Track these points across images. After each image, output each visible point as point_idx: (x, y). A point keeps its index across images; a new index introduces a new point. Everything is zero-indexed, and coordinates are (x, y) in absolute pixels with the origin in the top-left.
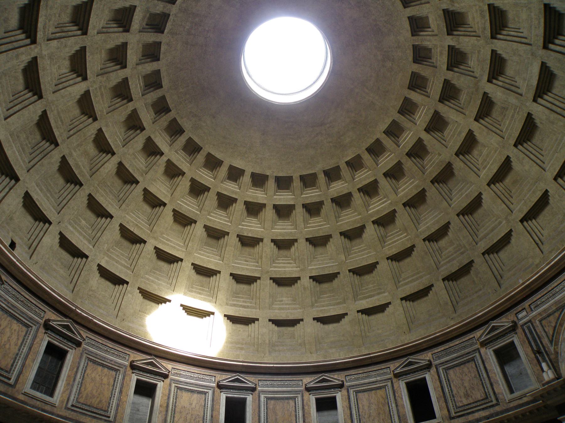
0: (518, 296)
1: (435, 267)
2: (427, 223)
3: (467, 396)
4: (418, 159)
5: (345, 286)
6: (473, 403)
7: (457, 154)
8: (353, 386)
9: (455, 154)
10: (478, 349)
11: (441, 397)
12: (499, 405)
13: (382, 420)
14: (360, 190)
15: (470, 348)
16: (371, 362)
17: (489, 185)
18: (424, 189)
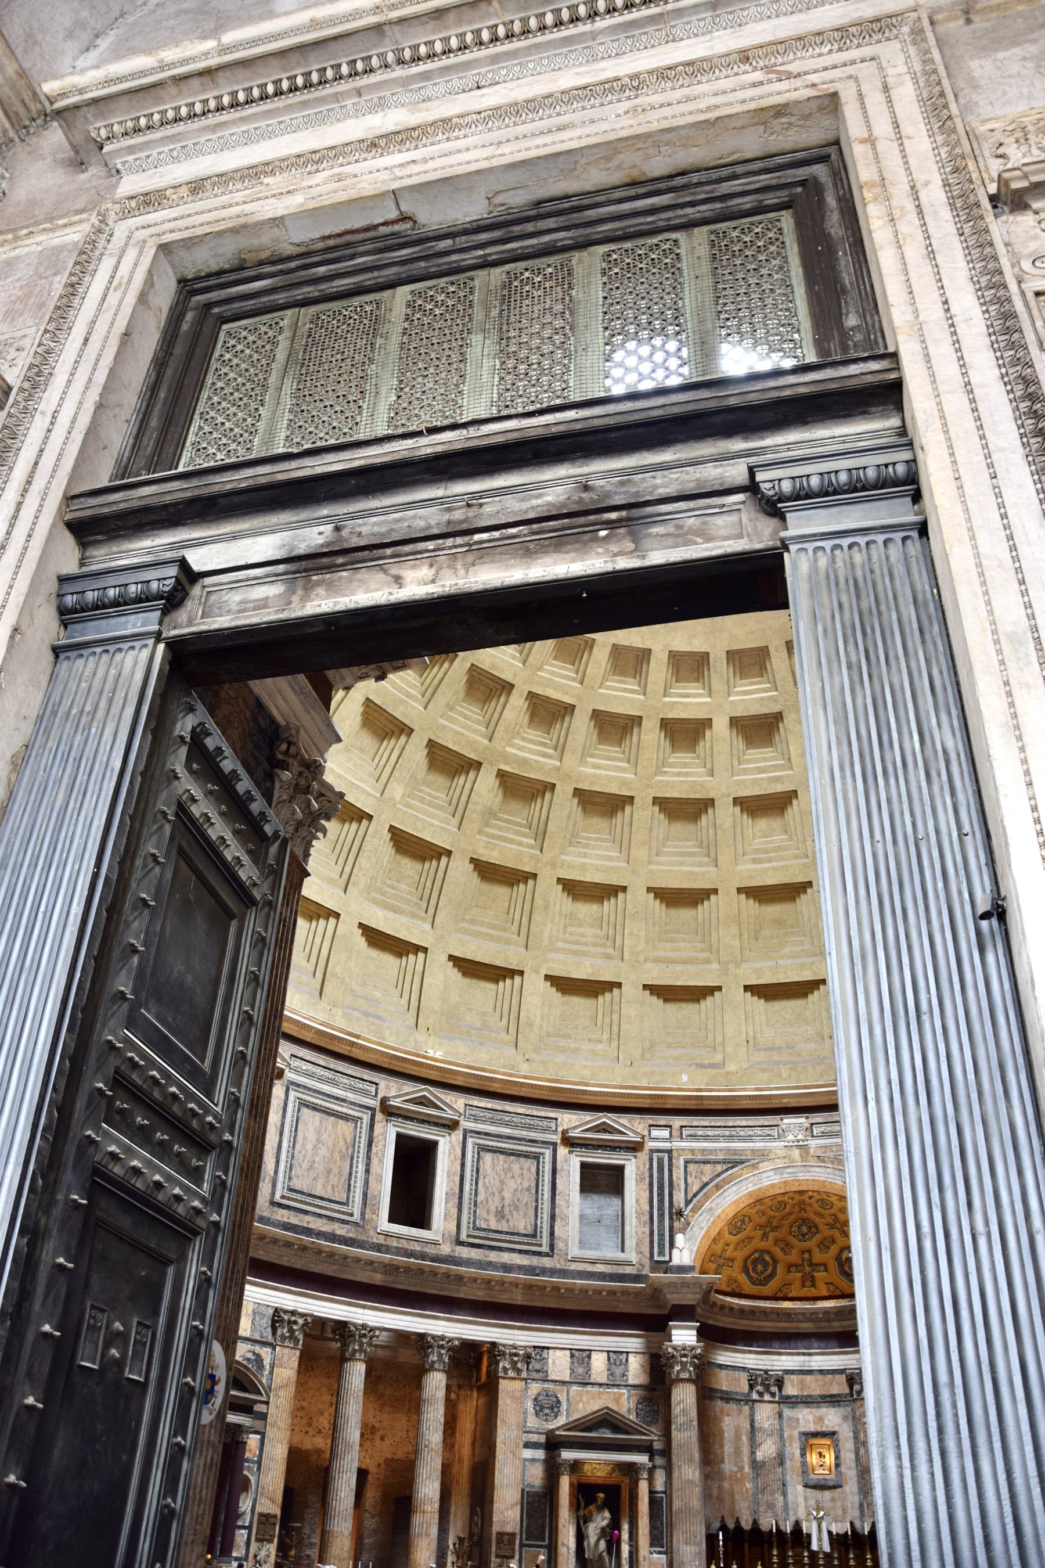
0: (673, 1101)
1: (546, 943)
2: (585, 856)
3: (500, 1215)
4: (668, 743)
5: (366, 855)
6: (507, 1233)
7: (737, 801)
8: (298, 1085)
9: (734, 799)
10: (555, 1144)
11: (453, 1195)
12: (552, 1256)
13: (330, 1188)
14: (532, 697)
15: (541, 1135)
16: (347, 1053)
17: (740, 890)
18: (632, 798)
